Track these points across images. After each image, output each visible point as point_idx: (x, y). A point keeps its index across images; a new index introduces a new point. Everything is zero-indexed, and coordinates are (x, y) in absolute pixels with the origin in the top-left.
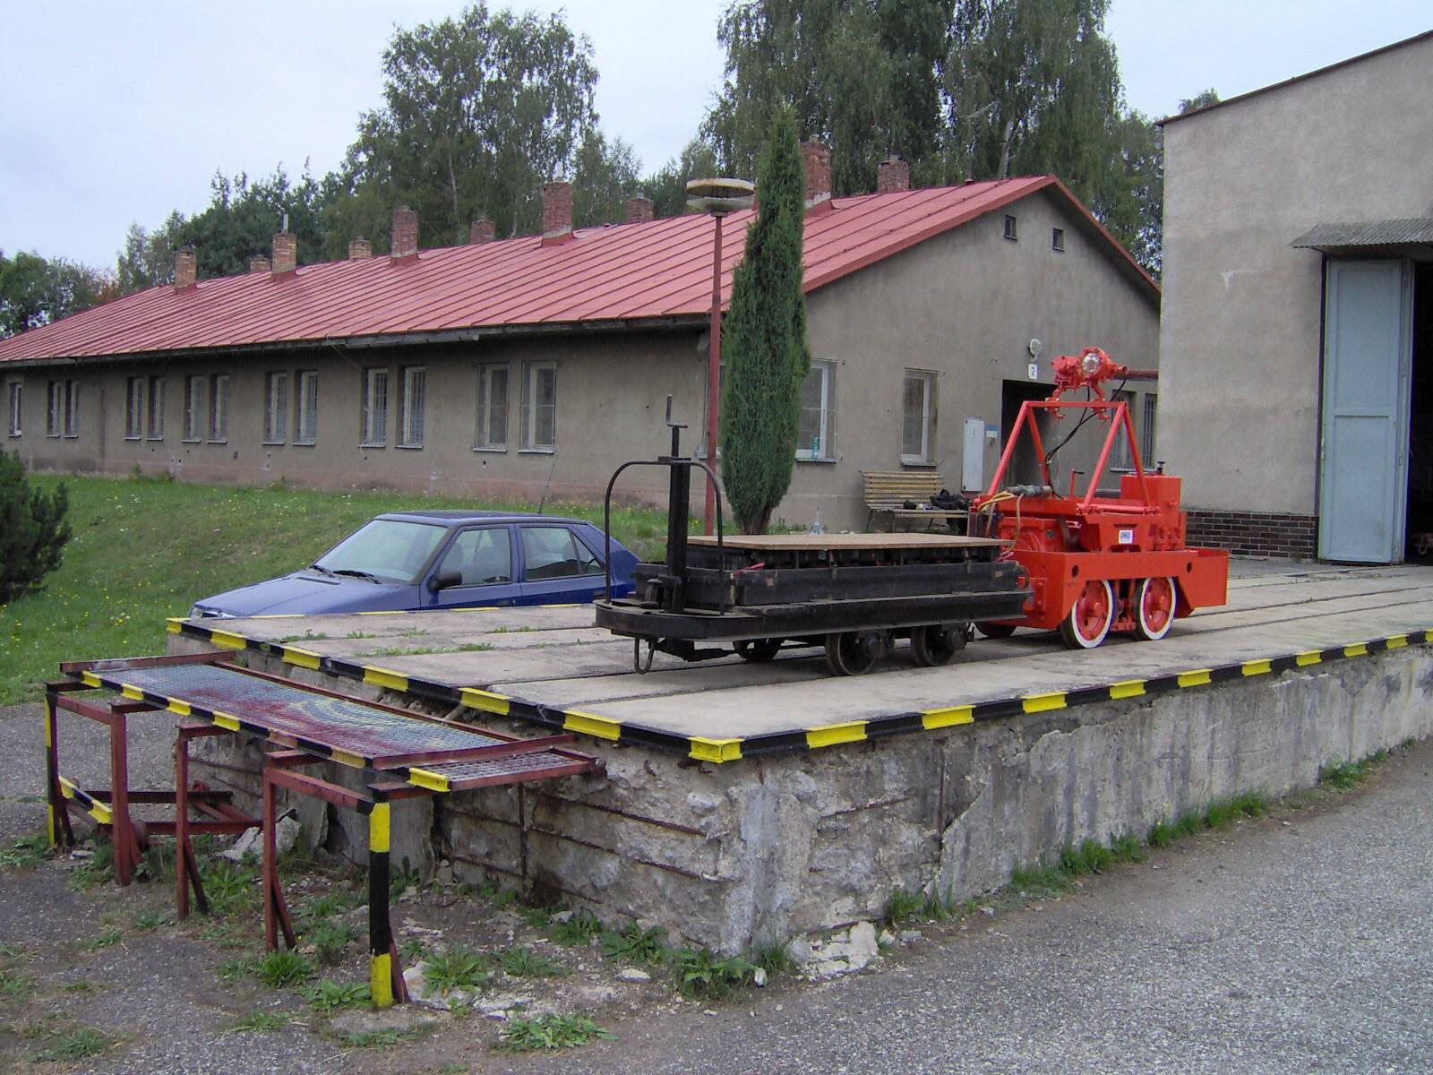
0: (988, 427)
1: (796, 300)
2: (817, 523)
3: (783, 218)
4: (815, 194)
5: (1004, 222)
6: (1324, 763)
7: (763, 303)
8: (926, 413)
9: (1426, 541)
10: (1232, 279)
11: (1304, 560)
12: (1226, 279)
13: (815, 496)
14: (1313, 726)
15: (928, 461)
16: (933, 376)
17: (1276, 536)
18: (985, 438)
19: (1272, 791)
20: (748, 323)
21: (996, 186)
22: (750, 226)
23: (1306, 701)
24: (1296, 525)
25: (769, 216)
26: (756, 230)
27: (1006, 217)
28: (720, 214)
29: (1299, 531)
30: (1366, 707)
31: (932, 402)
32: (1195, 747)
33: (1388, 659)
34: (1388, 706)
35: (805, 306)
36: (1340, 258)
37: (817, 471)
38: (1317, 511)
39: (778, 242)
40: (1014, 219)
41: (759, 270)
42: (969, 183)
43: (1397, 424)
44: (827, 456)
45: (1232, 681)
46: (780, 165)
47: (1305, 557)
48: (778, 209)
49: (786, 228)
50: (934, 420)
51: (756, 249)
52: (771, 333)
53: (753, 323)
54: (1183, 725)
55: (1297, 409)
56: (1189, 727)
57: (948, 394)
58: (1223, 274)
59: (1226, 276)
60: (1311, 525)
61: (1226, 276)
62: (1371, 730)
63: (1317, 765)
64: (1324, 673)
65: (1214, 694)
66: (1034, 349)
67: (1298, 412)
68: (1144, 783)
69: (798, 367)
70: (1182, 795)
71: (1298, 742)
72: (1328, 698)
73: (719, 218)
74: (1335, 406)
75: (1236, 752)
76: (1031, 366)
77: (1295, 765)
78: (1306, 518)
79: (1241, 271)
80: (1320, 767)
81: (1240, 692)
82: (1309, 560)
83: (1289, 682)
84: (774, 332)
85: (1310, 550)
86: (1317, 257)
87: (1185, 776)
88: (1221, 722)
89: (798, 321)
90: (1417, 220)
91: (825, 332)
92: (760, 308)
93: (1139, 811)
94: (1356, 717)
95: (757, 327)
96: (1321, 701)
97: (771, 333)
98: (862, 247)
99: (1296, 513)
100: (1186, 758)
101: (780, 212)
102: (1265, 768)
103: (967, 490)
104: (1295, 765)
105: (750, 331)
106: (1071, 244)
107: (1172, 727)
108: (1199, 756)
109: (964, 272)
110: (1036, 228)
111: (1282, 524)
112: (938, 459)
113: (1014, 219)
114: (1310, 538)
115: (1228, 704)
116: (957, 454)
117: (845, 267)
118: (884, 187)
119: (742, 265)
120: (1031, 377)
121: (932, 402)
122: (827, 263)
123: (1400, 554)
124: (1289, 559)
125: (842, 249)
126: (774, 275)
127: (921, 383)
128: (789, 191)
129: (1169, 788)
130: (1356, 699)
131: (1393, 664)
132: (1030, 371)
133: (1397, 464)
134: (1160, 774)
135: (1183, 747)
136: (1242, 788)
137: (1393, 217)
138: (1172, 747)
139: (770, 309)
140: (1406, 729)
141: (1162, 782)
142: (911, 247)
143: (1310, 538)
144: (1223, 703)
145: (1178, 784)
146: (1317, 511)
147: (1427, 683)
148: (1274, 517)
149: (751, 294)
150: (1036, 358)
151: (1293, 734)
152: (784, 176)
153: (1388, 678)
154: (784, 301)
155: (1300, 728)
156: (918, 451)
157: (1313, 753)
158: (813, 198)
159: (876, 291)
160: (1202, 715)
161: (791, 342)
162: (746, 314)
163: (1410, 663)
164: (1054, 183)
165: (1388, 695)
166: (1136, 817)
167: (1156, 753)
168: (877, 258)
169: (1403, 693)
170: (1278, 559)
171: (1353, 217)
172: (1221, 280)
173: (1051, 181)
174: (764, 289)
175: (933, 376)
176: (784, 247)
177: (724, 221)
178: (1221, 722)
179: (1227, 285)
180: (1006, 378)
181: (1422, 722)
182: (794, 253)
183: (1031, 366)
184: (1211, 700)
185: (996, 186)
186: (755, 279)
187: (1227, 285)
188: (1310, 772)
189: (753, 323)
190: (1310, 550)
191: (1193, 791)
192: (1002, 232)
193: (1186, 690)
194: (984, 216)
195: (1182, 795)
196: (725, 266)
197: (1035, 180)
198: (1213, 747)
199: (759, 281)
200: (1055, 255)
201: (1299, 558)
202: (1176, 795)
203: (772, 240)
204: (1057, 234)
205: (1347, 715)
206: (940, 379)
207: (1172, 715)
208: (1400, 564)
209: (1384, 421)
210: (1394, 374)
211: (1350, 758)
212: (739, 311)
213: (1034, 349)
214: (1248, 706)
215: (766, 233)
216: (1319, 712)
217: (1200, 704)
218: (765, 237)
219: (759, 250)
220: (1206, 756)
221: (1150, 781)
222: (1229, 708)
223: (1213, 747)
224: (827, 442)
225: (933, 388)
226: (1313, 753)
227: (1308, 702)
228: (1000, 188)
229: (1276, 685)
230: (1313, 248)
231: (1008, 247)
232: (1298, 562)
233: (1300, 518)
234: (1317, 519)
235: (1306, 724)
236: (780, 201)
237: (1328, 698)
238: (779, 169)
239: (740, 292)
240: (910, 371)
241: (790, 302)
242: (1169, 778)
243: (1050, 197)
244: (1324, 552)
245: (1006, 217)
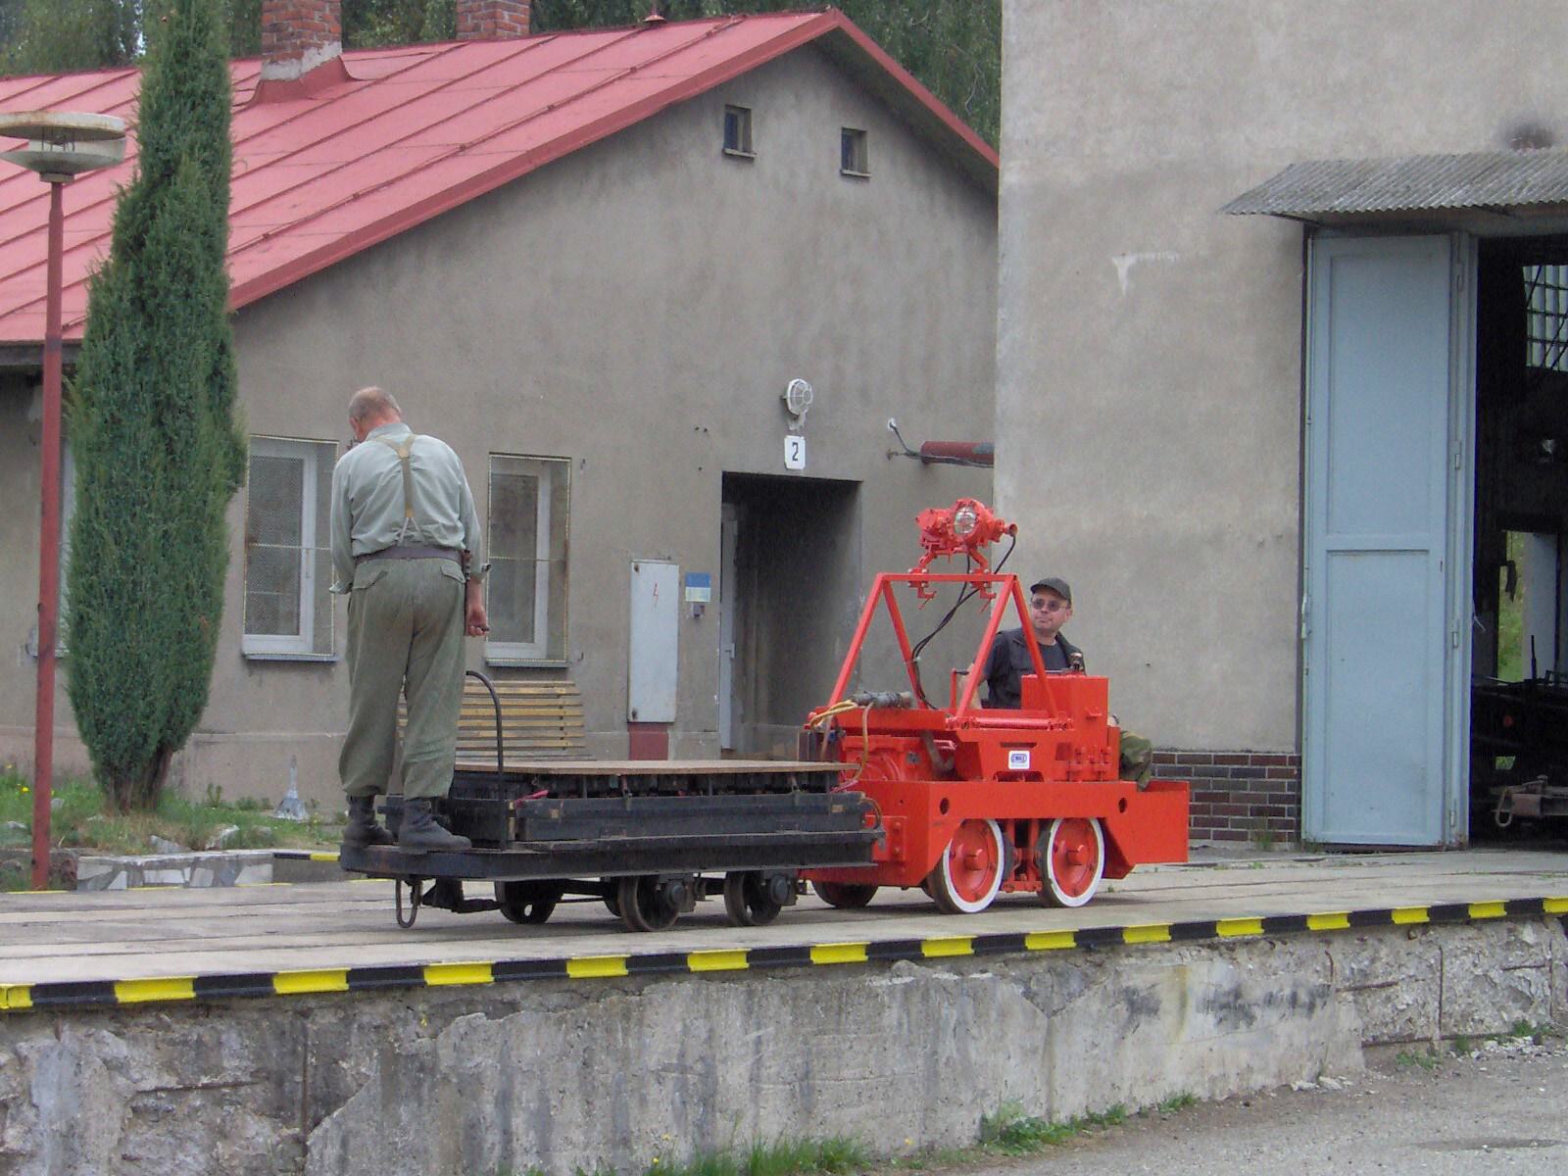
0: (689, 580)
1: (213, 341)
2: (293, 794)
3: (187, 179)
4: (304, 46)
5: (722, 119)
6: (990, 1115)
7: (147, 347)
8: (543, 550)
9: (1508, 798)
10: (1132, 272)
11: (1277, 846)
12: (1122, 273)
13: (286, 735)
14: (963, 1051)
15: (549, 657)
16: (557, 467)
17: (1225, 797)
18: (682, 603)
19: (883, 1145)
20: (118, 388)
21: (709, 35)
22: (123, 193)
23: (944, 1012)
24: (1260, 774)
25: (160, 172)
26: (135, 202)
27: (727, 109)
28: (58, 178)
29: (1265, 786)
30: (1082, 1034)
31: (558, 525)
32: (724, 1061)
33: (1132, 960)
34: (1130, 1038)
35: (233, 349)
36: (1337, 236)
37: (294, 680)
38: (1299, 747)
39: (177, 229)
40: (747, 111)
41: (139, 281)
42: (654, 25)
43: (1447, 566)
44: (316, 649)
45: (791, 971)
46: (180, 72)
47: (1279, 838)
48: (178, 162)
49: (192, 199)
50: (561, 567)
51: (134, 236)
52: (163, 407)
53: (129, 388)
54: (701, 1028)
55: (1260, 538)
56: (711, 1030)
57: (590, 506)
58: (1116, 261)
59: (1123, 265)
60: (1288, 774)
61: (1123, 265)
62: (1095, 1073)
63: (977, 1116)
64: (983, 972)
65: (757, 986)
66: (799, 401)
67: (1261, 544)
68: (633, 1103)
69: (219, 474)
70: (703, 1128)
71: (933, 1076)
72: (993, 1015)
73: (57, 187)
74: (1328, 531)
75: (806, 1075)
76: (789, 440)
77: (929, 1110)
78: (1280, 760)
79: (1150, 256)
80: (984, 1119)
81: (808, 987)
82: (1287, 845)
83: (907, 980)
84: (169, 404)
85: (1287, 825)
86: (1295, 230)
87: (708, 1101)
88: (771, 1029)
89: (219, 381)
90: (1476, 156)
91: (279, 392)
92: (141, 360)
93: (626, 1142)
94: (1059, 1050)
95: (135, 394)
96: (978, 1015)
97: (163, 407)
98: (395, 188)
99: (1262, 748)
100: (708, 1075)
101: (182, 169)
102: (863, 1108)
103: (641, 718)
104: (929, 1110)
105: (122, 404)
106: (884, 160)
107: (679, 1027)
108: (734, 1076)
109: (626, 236)
110: (799, 131)
111: (1237, 774)
112: (571, 652)
113: (747, 111)
114: (1288, 799)
115: (784, 1003)
116: (616, 639)
117: (350, 238)
118: (470, 22)
119: (106, 272)
120: (791, 464)
121: (558, 525)
122: (312, 228)
123: (1460, 827)
124: (1249, 844)
125: (348, 193)
126: (168, 292)
127: (530, 487)
128: (200, 122)
129: (680, 1117)
130: (1056, 1019)
131: (1139, 969)
132: (789, 450)
133: (1448, 648)
134: (662, 1098)
135: (702, 1059)
136: (818, 1135)
137: (1435, 149)
138: (682, 1055)
139: (161, 361)
140: (1176, 1078)
141: (666, 1106)
142: (499, 190)
143: (1288, 799)
144: (775, 1000)
145: (695, 1112)
146: (1299, 747)
147: (1223, 1007)
148: (1220, 760)
149: (124, 330)
150: (802, 421)
151: (920, 1062)
152: (192, 93)
153: (1127, 990)
154: (190, 343)
155: (935, 1053)
156: (526, 634)
157: (966, 1096)
158: (299, 56)
159: (426, 286)
160: (736, 1019)
161: (204, 424)
162: (114, 371)
163: (1180, 971)
164: (837, 32)
165: (1130, 1020)
166: (620, 1151)
167: (652, 1062)
168: (425, 216)
169: (1167, 1020)
170: (1229, 845)
171: (1361, 147)
172: (1112, 272)
173: (831, 24)
174: (150, 321)
175: (557, 467)
176: (185, 236)
177: (67, 193)
178: (771, 1029)
179: (1124, 285)
180: (734, 467)
181: (1215, 1071)
182: (210, 248)
183: (789, 440)
184: (750, 994)
185: (709, 35)
186: (132, 302)
187: (1124, 285)
188: (961, 1125)
189: (129, 388)
190: (1287, 825)
191: (722, 1124)
192: (718, 142)
193: (706, 976)
194: (670, 113)
195: (703, 1128)
196: (75, 268)
197: (798, 20)
198: (758, 1063)
199: (140, 304)
200: (848, 190)
201: (1267, 842)
202: (691, 1128)
203: (164, 223)
204: (851, 141)
205: (1040, 1043)
206: (574, 476)
207: (678, 1010)
208: (1461, 848)
209: (1423, 557)
210: (1439, 474)
211: (1050, 1113)
212: (99, 365)
213: (799, 401)
214: (825, 1010)
215: (153, 208)
216: (974, 1031)
217: (733, 998)
218: (153, 217)
219: (139, 243)
220: (747, 1076)
221: (643, 1101)
222: (787, 1009)
223: (758, 1063)
224: (317, 616)
225: (559, 495)
226: (966, 1096)
227: (950, 1014)
228: (718, 41)
229: (880, 982)
230: (1282, 215)
231: (730, 176)
232: (1267, 849)
233: (1265, 760)
234: (1297, 761)
235: (949, 1047)
236: (182, 143)
237: (993, 1015)
238: (180, 80)
239: (102, 325)
240: (500, 458)
241: (201, 346)
242: (678, 1100)
243: (829, 58)
244: (1314, 827)
245: (727, 109)
